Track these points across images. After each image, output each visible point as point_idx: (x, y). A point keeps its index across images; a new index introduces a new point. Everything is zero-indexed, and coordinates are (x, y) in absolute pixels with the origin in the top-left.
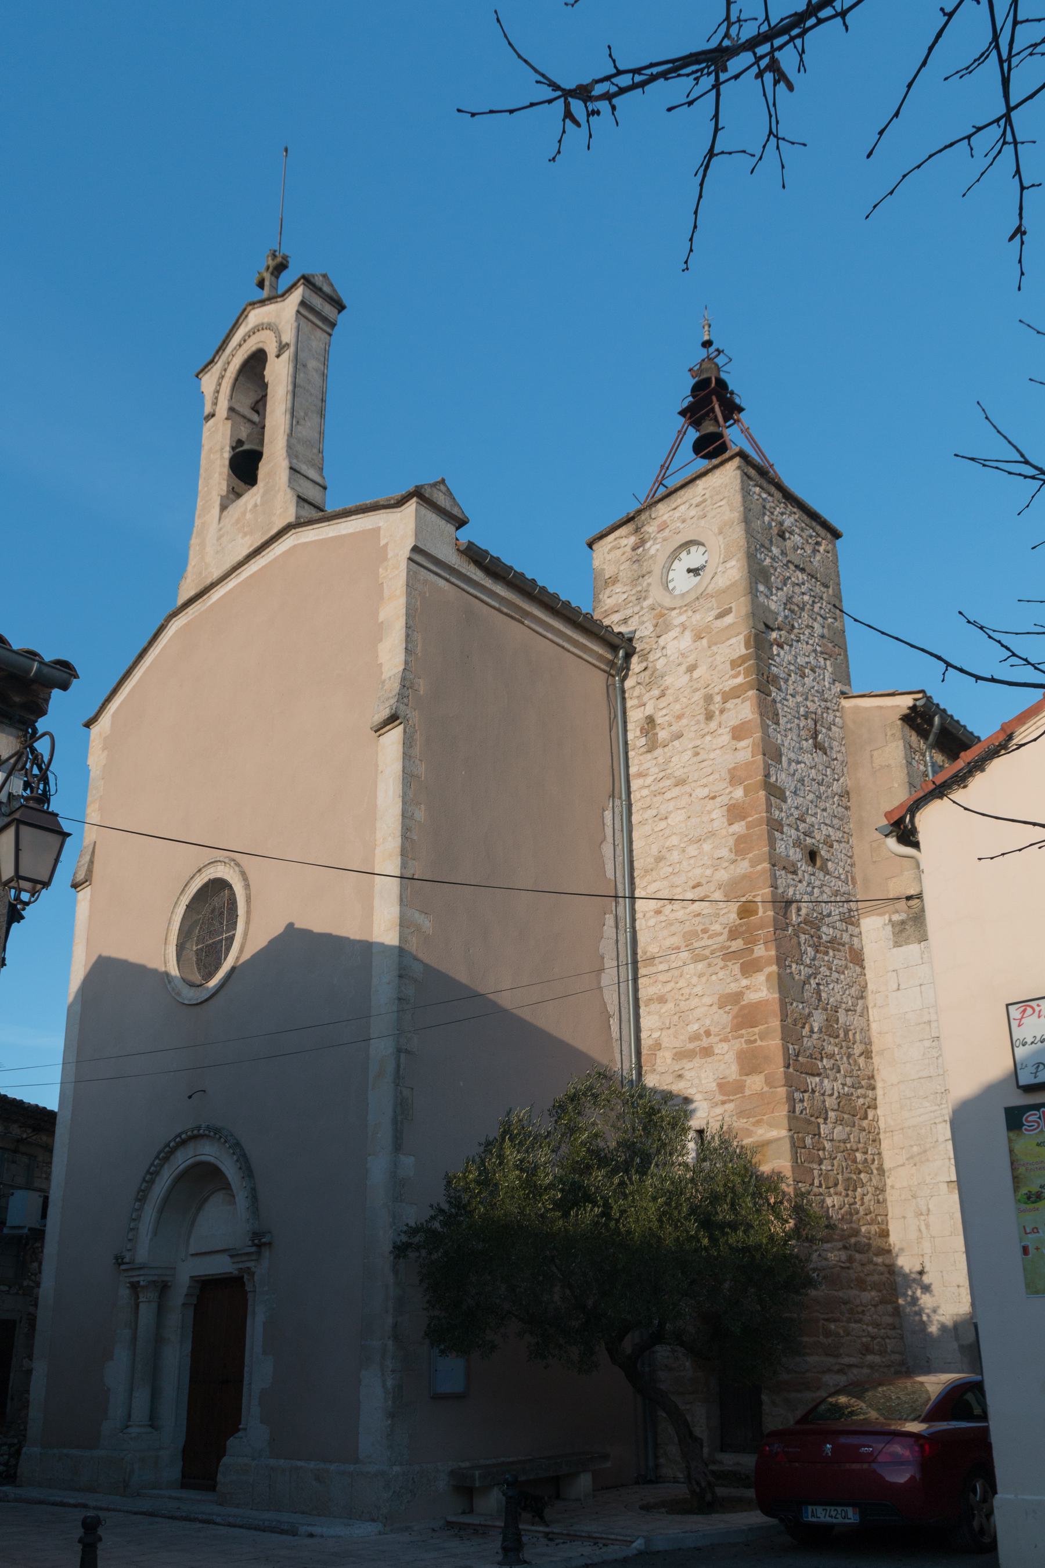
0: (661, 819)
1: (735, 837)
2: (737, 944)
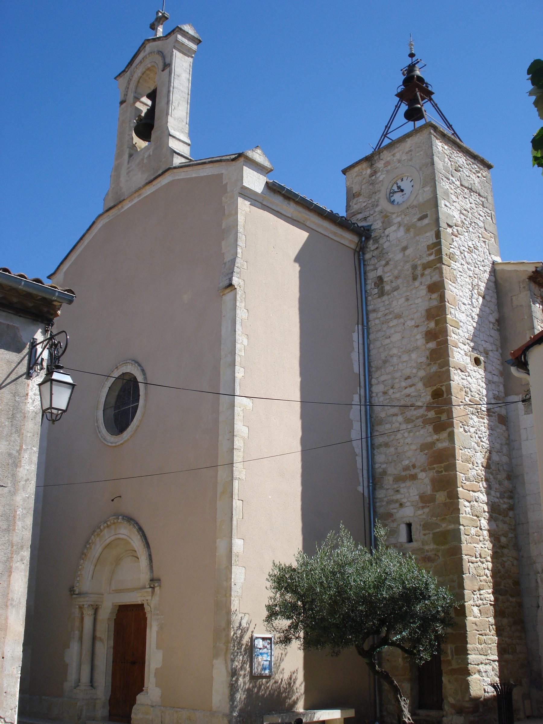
0: (386, 338)
1: (430, 350)
2: (431, 414)
